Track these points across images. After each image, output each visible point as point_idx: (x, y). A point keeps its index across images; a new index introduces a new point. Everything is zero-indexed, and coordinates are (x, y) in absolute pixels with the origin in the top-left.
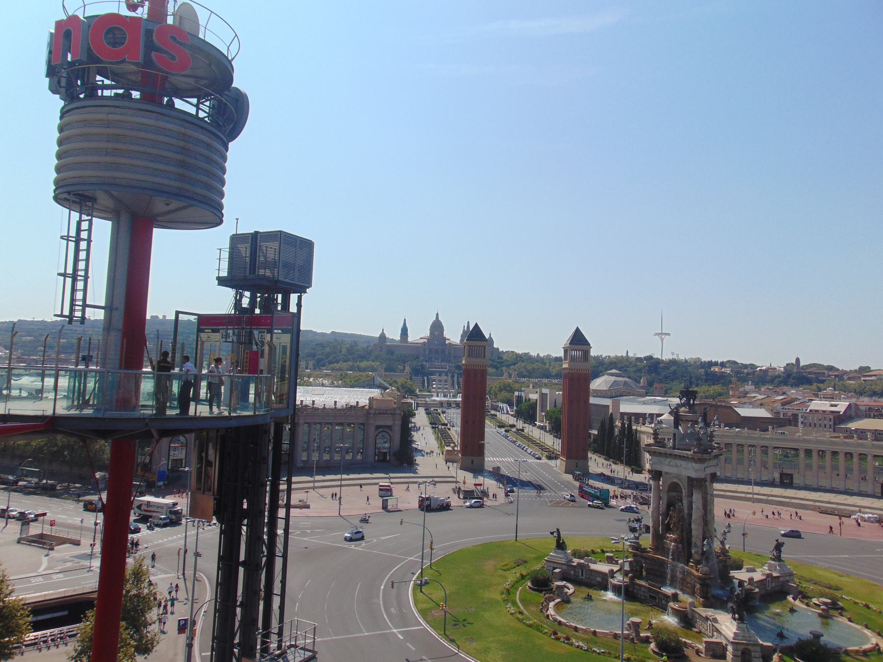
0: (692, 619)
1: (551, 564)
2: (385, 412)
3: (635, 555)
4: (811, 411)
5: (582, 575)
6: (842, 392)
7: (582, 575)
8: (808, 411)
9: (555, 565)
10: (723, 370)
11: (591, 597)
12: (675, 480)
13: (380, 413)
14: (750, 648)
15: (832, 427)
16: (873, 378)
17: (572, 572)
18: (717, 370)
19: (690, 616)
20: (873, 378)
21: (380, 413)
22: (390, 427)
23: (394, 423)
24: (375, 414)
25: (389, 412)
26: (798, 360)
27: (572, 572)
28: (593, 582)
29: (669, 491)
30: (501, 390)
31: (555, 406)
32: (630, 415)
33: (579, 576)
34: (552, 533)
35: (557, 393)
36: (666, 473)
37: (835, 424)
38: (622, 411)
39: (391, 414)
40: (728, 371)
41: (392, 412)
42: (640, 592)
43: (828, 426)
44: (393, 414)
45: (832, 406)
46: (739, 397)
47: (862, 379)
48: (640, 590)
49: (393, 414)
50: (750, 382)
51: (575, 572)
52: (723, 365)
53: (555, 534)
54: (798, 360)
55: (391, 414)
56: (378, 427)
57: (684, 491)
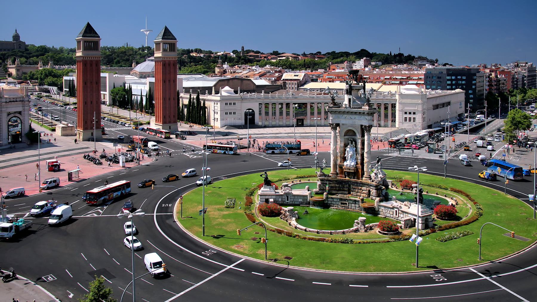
0: (378, 211)
1: (264, 197)
2: (15, 100)
3: (321, 180)
4: (283, 79)
5: (288, 200)
6: (275, 67)
7: (288, 200)
8: (282, 79)
9: (267, 197)
10: (198, 55)
11: (307, 212)
12: (351, 129)
13: (10, 102)
14: (428, 217)
15: (297, 88)
16: (284, 58)
17: (280, 200)
18: (194, 55)
19: (377, 209)
20: (284, 58)
21: (10, 102)
22: (20, 113)
23: (24, 109)
24: (6, 102)
25: (18, 100)
26: (243, 47)
27: (280, 200)
28: (296, 203)
29: (344, 136)
30: (46, 76)
31: (114, 87)
32: (195, 90)
33: (285, 201)
34: (261, 176)
35: (114, 76)
36: (343, 124)
37: (298, 87)
38: (183, 86)
39: (20, 101)
40: (202, 55)
41: (21, 99)
42: (333, 202)
43: (294, 88)
44: (22, 101)
45: (295, 76)
46: (231, 73)
47: (278, 58)
48: (333, 201)
49: (22, 101)
50: (226, 62)
51: (282, 198)
52: (197, 51)
53: (264, 176)
54: (243, 47)
55: (20, 101)
56: (9, 114)
57: (357, 134)
